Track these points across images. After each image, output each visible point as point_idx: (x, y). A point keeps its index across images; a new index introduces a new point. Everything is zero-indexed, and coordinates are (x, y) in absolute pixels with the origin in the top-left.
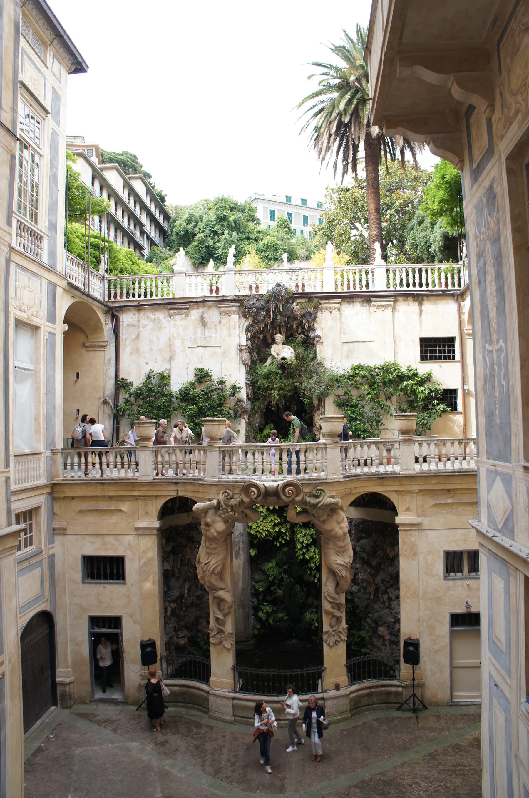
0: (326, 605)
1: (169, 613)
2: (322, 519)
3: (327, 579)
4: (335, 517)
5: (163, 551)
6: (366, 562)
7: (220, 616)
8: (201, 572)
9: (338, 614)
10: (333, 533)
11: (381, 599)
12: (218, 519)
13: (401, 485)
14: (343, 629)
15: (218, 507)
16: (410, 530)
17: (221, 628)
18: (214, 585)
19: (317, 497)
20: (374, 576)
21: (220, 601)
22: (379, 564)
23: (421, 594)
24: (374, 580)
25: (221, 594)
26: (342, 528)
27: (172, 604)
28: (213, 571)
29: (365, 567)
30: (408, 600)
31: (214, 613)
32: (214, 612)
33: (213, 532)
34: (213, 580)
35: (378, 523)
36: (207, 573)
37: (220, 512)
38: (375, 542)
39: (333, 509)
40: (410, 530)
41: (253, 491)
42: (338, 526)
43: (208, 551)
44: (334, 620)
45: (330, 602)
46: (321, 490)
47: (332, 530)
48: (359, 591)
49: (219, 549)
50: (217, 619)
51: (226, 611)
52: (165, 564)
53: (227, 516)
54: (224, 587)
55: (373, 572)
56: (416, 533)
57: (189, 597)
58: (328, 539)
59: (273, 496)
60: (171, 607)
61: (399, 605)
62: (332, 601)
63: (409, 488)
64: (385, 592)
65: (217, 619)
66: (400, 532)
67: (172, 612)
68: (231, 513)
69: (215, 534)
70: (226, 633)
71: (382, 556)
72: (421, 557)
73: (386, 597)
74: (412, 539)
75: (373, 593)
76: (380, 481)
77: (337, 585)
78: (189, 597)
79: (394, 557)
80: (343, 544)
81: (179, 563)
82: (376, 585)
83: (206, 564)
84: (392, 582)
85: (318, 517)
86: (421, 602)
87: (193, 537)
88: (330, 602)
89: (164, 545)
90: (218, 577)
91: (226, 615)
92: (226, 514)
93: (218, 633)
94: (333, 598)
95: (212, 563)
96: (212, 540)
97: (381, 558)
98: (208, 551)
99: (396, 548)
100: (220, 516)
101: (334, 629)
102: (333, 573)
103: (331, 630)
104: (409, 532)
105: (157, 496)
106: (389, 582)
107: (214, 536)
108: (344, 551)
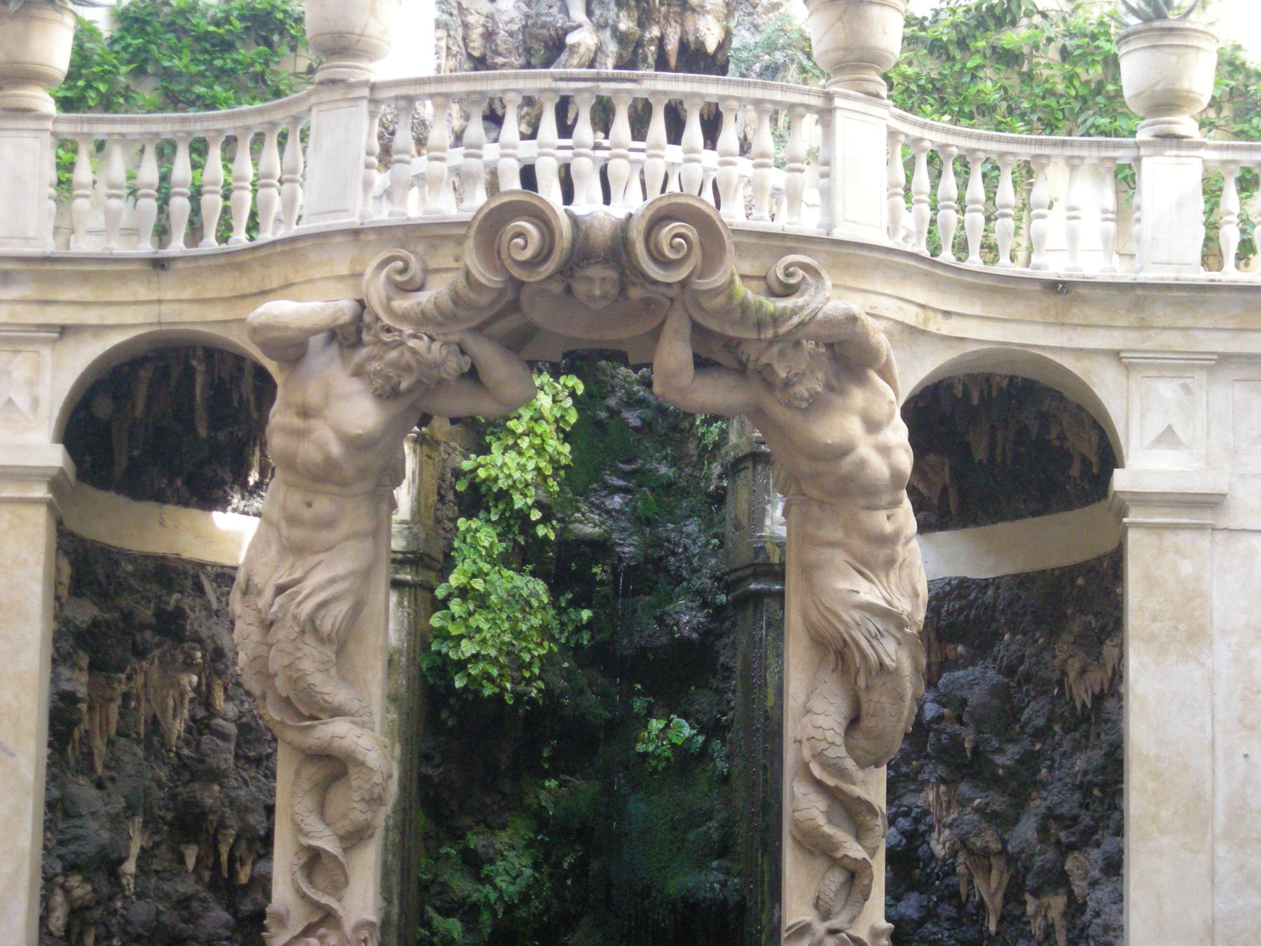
0: (803, 804)
1: (58, 920)
2: (801, 390)
3: (810, 694)
4: (858, 397)
5: (56, 618)
6: (966, 767)
7: (328, 843)
8: (255, 633)
9: (855, 850)
10: (847, 464)
11: (1037, 927)
12: (355, 385)
13: (1144, 327)
14: (876, 934)
15: (347, 336)
16: (1175, 527)
17: (325, 900)
18: (309, 693)
19: (788, 291)
20: (1003, 821)
21: (333, 767)
22: (1029, 761)
23: (1220, 817)
24: (1004, 843)
25: (338, 732)
26: (884, 450)
27: (75, 880)
28: (312, 619)
29: (964, 788)
30: (1166, 840)
31: (297, 821)
32: (298, 829)
33: (324, 441)
34: (306, 665)
35: (1022, 581)
36: (281, 634)
37: (364, 352)
38: (1010, 671)
39: (848, 355)
40: (1175, 527)
41: (520, 234)
42: (871, 439)
43: (298, 534)
44: (836, 879)
45: (819, 785)
46: (805, 267)
47: (843, 451)
48: (929, 914)
49: (344, 528)
50: (313, 860)
51: (359, 814)
52: (65, 672)
53: (394, 365)
54: (354, 705)
55: (999, 802)
56: (1204, 542)
57: (140, 896)
58: (821, 503)
59: (605, 261)
60: (67, 891)
61: (1119, 898)
62: (831, 781)
63: (1174, 340)
64: (1061, 880)
65: (313, 860)
66: (1132, 536)
67: (68, 929)
68: (412, 343)
69: (336, 449)
70: (348, 925)
71: (1041, 722)
72: (1221, 655)
73: (1057, 903)
74: (1186, 568)
75: (994, 904)
76: (1050, 301)
77: (854, 722)
78: (140, 896)
79: (1098, 698)
80: (889, 528)
81: (114, 709)
82: (1011, 859)
83: (281, 590)
84: (1086, 819)
85: (787, 384)
86: (1221, 850)
87: (179, 614)
88: (819, 785)
89: (64, 592)
90: (330, 652)
91: (354, 838)
92: (393, 355)
93: (308, 931)
94: (841, 773)
95: (309, 584)
96: (322, 476)
97: (1039, 734)
98: (298, 534)
99: (1109, 650)
100: (358, 373)
101: (835, 923)
102: (837, 653)
103: (820, 927)
104: (1170, 538)
105: (64, 331)
106: (1075, 819)
107: (328, 459)
108: (890, 563)
